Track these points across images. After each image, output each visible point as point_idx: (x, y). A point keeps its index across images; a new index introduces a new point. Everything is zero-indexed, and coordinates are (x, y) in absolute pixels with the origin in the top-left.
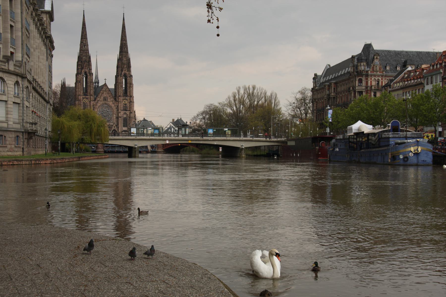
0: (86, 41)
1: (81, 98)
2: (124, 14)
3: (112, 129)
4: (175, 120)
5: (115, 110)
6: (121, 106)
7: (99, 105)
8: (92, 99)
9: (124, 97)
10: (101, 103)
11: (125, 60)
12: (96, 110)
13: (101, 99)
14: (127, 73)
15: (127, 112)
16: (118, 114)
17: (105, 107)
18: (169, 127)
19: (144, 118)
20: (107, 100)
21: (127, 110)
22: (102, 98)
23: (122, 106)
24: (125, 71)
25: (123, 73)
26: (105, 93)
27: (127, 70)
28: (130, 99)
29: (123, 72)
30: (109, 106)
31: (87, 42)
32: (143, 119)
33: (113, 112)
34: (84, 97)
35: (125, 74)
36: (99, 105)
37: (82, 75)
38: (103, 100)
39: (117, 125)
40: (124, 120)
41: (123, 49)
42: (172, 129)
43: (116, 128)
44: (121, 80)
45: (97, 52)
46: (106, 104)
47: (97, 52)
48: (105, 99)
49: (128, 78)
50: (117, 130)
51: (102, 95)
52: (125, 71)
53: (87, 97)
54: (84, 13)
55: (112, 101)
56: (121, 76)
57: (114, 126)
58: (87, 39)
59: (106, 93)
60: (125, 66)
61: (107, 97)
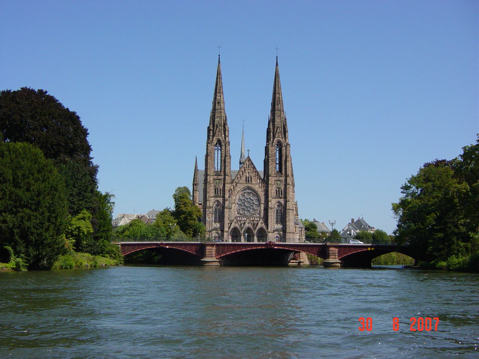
0: (220, 97)
1: (212, 179)
2: (277, 57)
3: (258, 227)
4: (355, 221)
6: (271, 190)
7: (238, 189)
8: (226, 181)
9: (277, 177)
10: (242, 186)
11: (278, 123)
12: (234, 198)
13: (241, 181)
14: (282, 140)
15: (282, 199)
17: (248, 193)
18: (347, 230)
19: (314, 219)
20: (251, 181)
21: (281, 198)
22: (244, 178)
23: (273, 192)
24: (279, 137)
25: (275, 141)
26: (247, 171)
27: (281, 137)
28: (286, 180)
29: (276, 139)
31: (222, 97)
33: (259, 200)
34: (215, 177)
35: (278, 142)
36: (239, 189)
37: (213, 144)
38: (245, 182)
39: (266, 221)
40: (277, 213)
41: (275, 106)
42: (352, 231)
43: (263, 224)
44: (272, 152)
46: (249, 188)
48: (248, 180)
49: (284, 148)
50: (265, 227)
51: (243, 174)
52: (279, 137)
53: (220, 177)
54: (219, 58)
55: (259, 184)
56: (272, 146)
57: (260, 221)
58: (223, 93)
59: (249, 171)
61: (251, 178)
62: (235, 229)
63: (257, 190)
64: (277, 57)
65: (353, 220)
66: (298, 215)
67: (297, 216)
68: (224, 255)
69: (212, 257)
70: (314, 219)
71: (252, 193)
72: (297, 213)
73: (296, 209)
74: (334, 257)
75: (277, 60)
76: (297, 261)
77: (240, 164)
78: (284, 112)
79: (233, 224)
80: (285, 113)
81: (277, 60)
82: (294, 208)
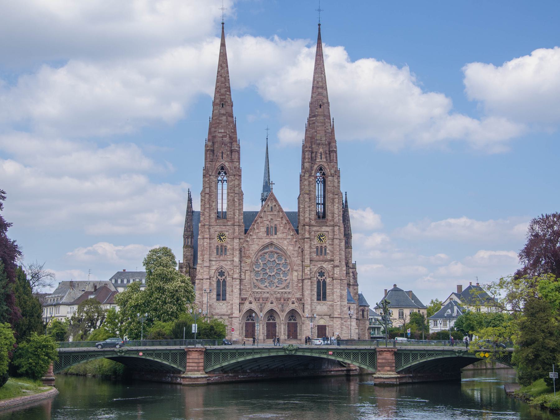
2: (319, 25)
5: (297, 260)
14: (325, 165)
16: (303, 271)
17: (272, 252)
18: (448, 305)
19: (395, 285)
22: (263, 229)
27: (325, 160)
30: (281, 253)
32: (392, 287)
42: (456, 308)
45: (267, 129)
46: (271, 244)
47: (267, 129)
60: (321, 150)
62: (251, 311)
63: (285, 248)
64: (319, 25)
65: (460, 287)
66: (357, 285)
67: (356, 288)
68: (218, 366)
69: (198, 371)
70: (395, 285)
71: (277, 253)
72: (356, 282)
73: (354, 275)
74: (388, 368)
75: (319, 30)
76: (345, 369)
77: (262, 201)
78: (330, 119)
79: (247, 303)
80: (332, 121)
81: (319, 30)
82: (351, 274)
